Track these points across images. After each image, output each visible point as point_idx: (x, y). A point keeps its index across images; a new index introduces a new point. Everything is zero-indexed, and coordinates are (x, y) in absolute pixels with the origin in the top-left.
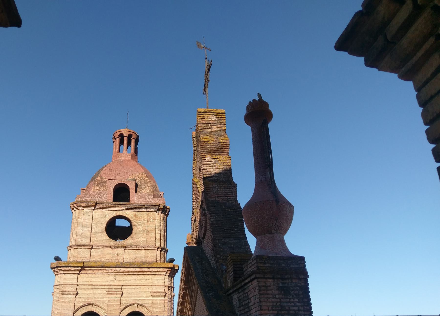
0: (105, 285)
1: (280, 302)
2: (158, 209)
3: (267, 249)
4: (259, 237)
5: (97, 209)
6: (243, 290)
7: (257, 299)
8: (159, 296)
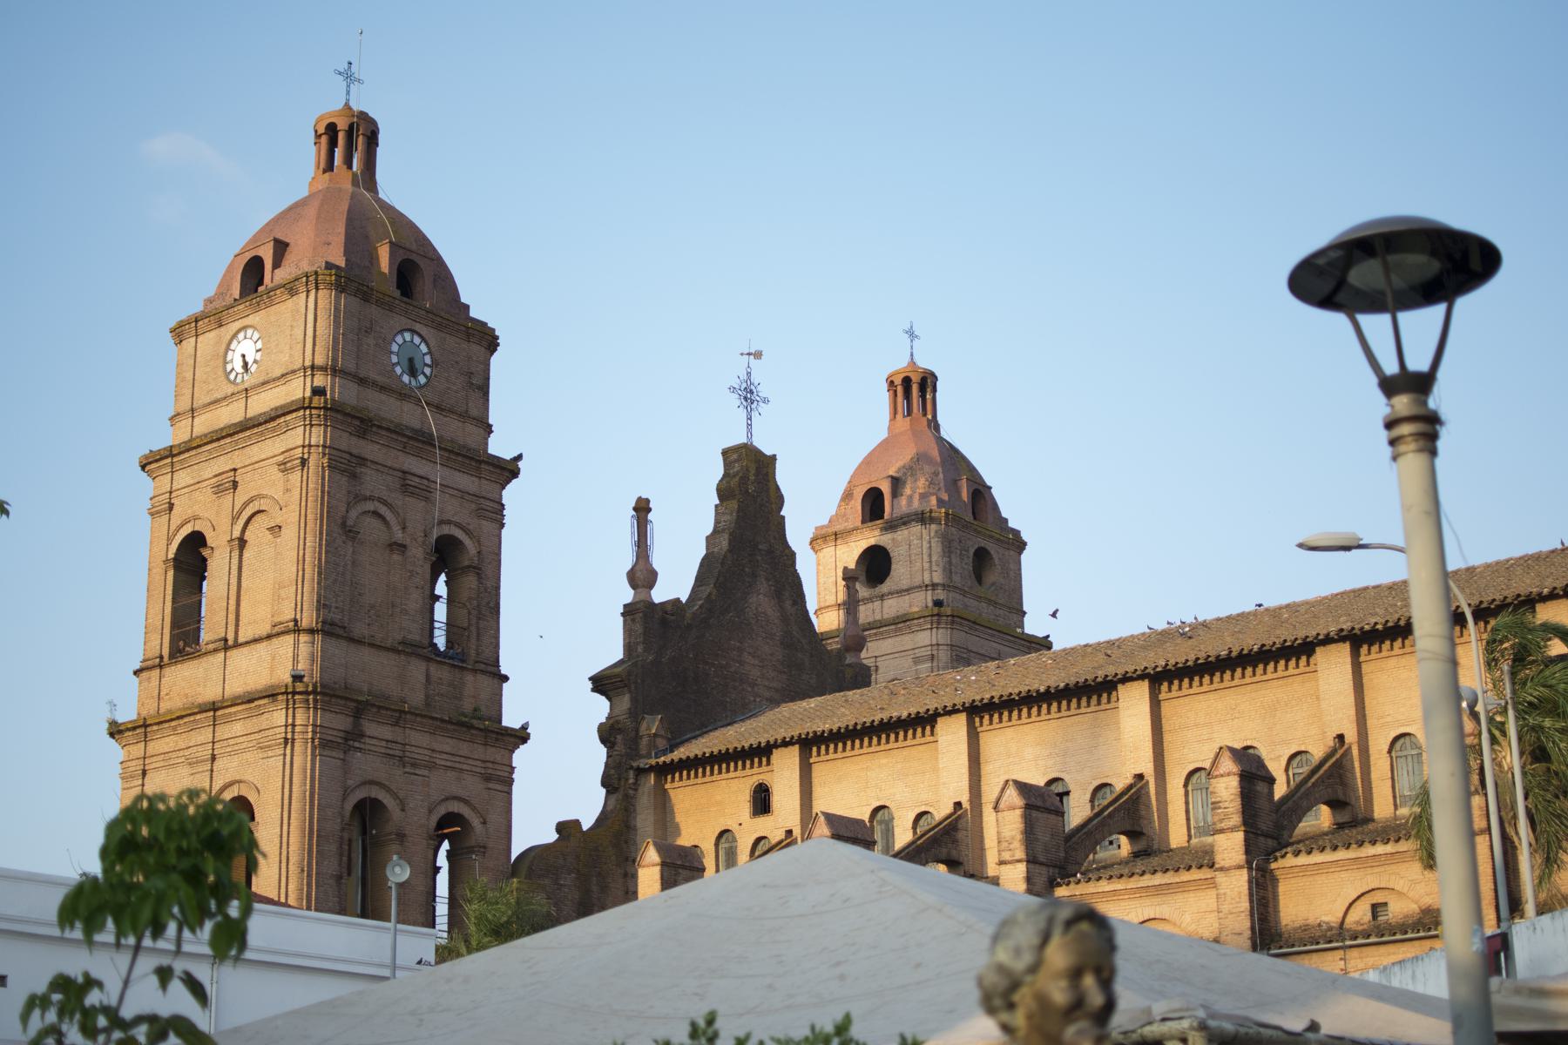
8: (923, 662)
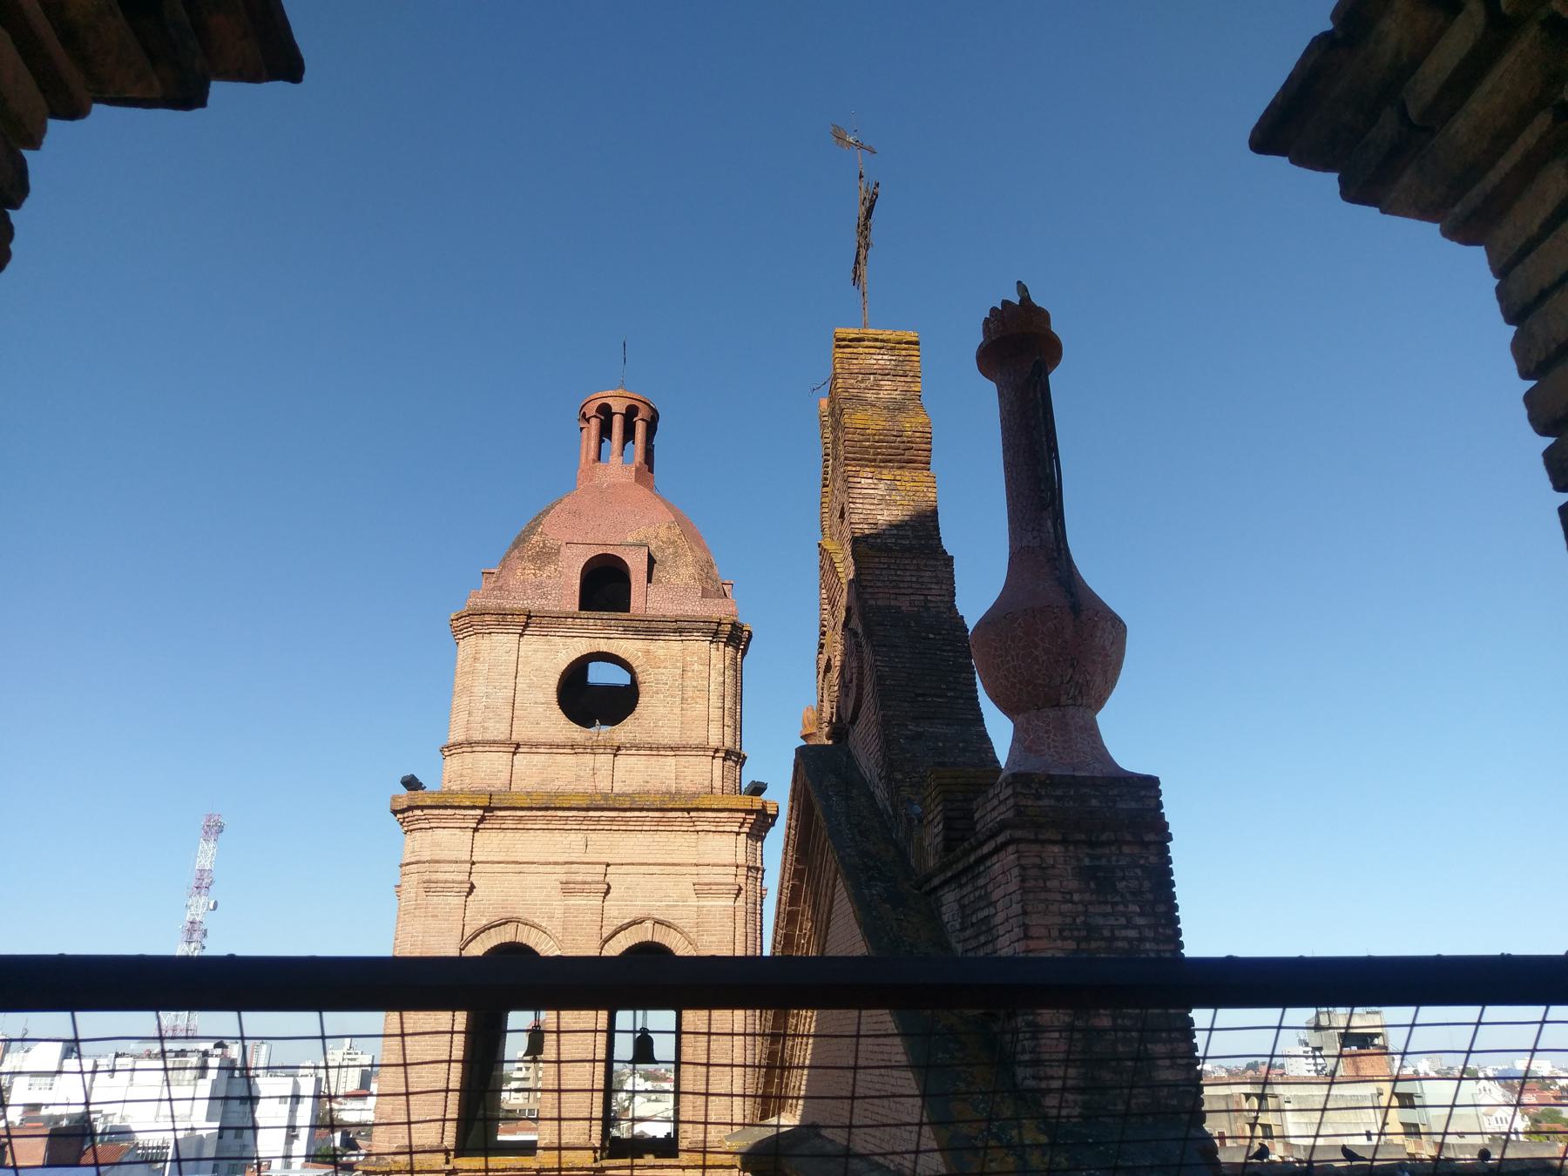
0: (556, 863)
1: (1086, 913)
2: (716, 634)
3: (1044, 755)
4: (1020, 718)
5: (531, 633)
6: (973, 878)
7: (1014, 905)
8: (718, 895)
